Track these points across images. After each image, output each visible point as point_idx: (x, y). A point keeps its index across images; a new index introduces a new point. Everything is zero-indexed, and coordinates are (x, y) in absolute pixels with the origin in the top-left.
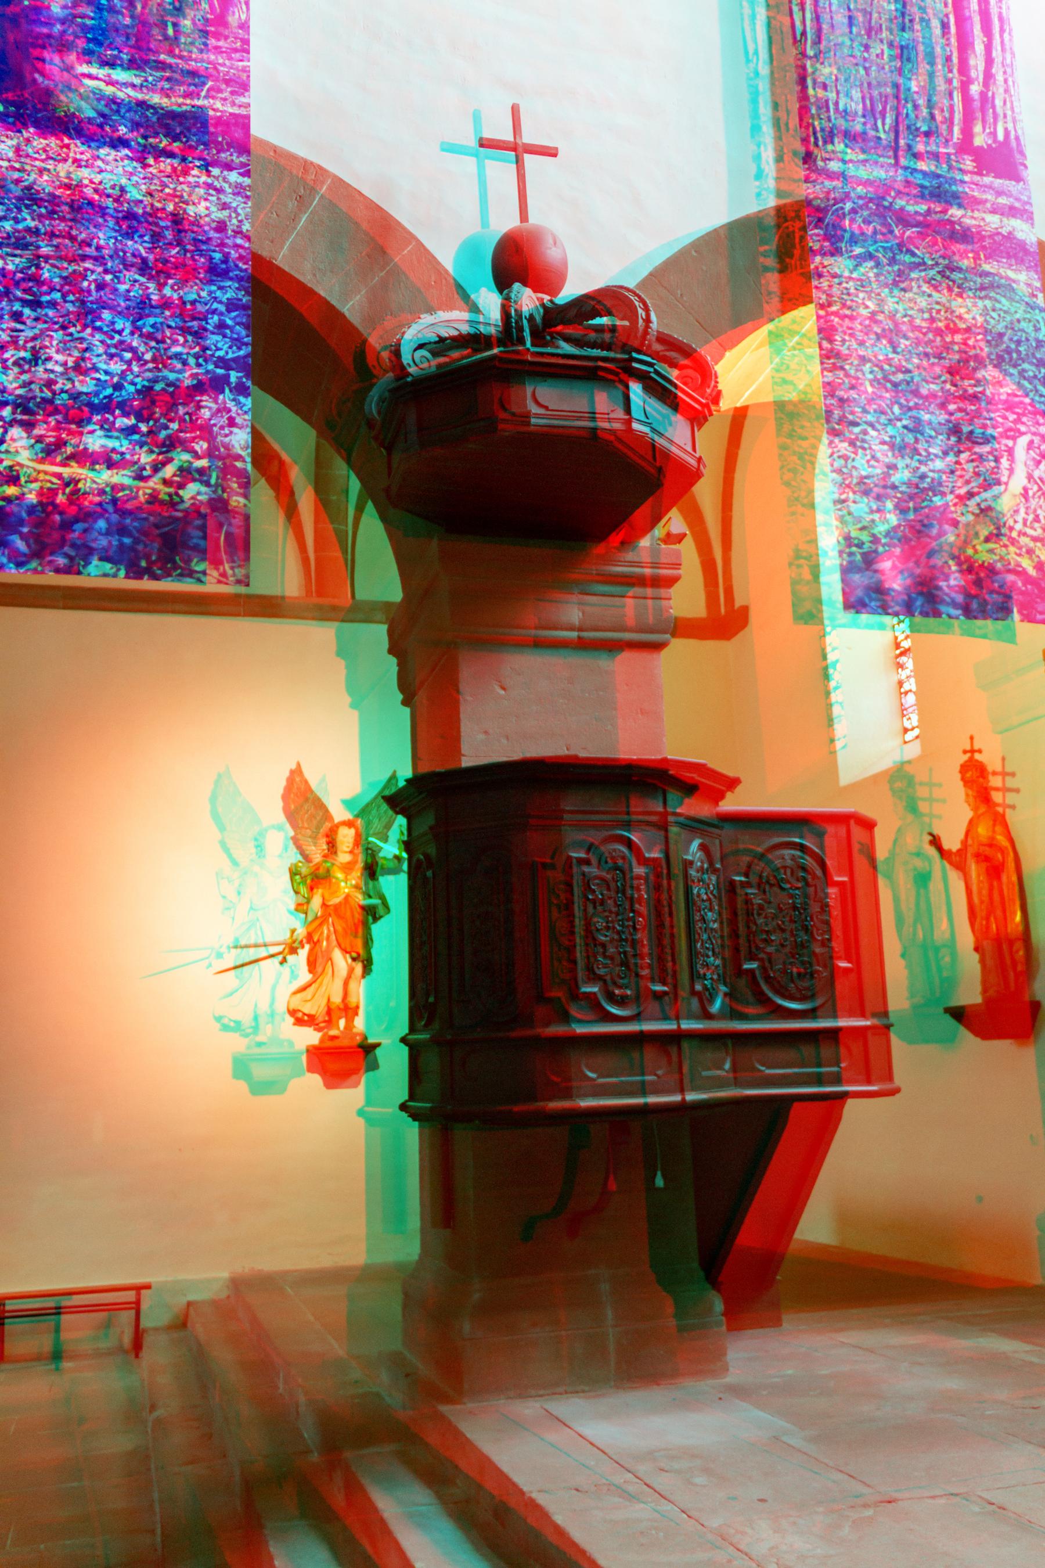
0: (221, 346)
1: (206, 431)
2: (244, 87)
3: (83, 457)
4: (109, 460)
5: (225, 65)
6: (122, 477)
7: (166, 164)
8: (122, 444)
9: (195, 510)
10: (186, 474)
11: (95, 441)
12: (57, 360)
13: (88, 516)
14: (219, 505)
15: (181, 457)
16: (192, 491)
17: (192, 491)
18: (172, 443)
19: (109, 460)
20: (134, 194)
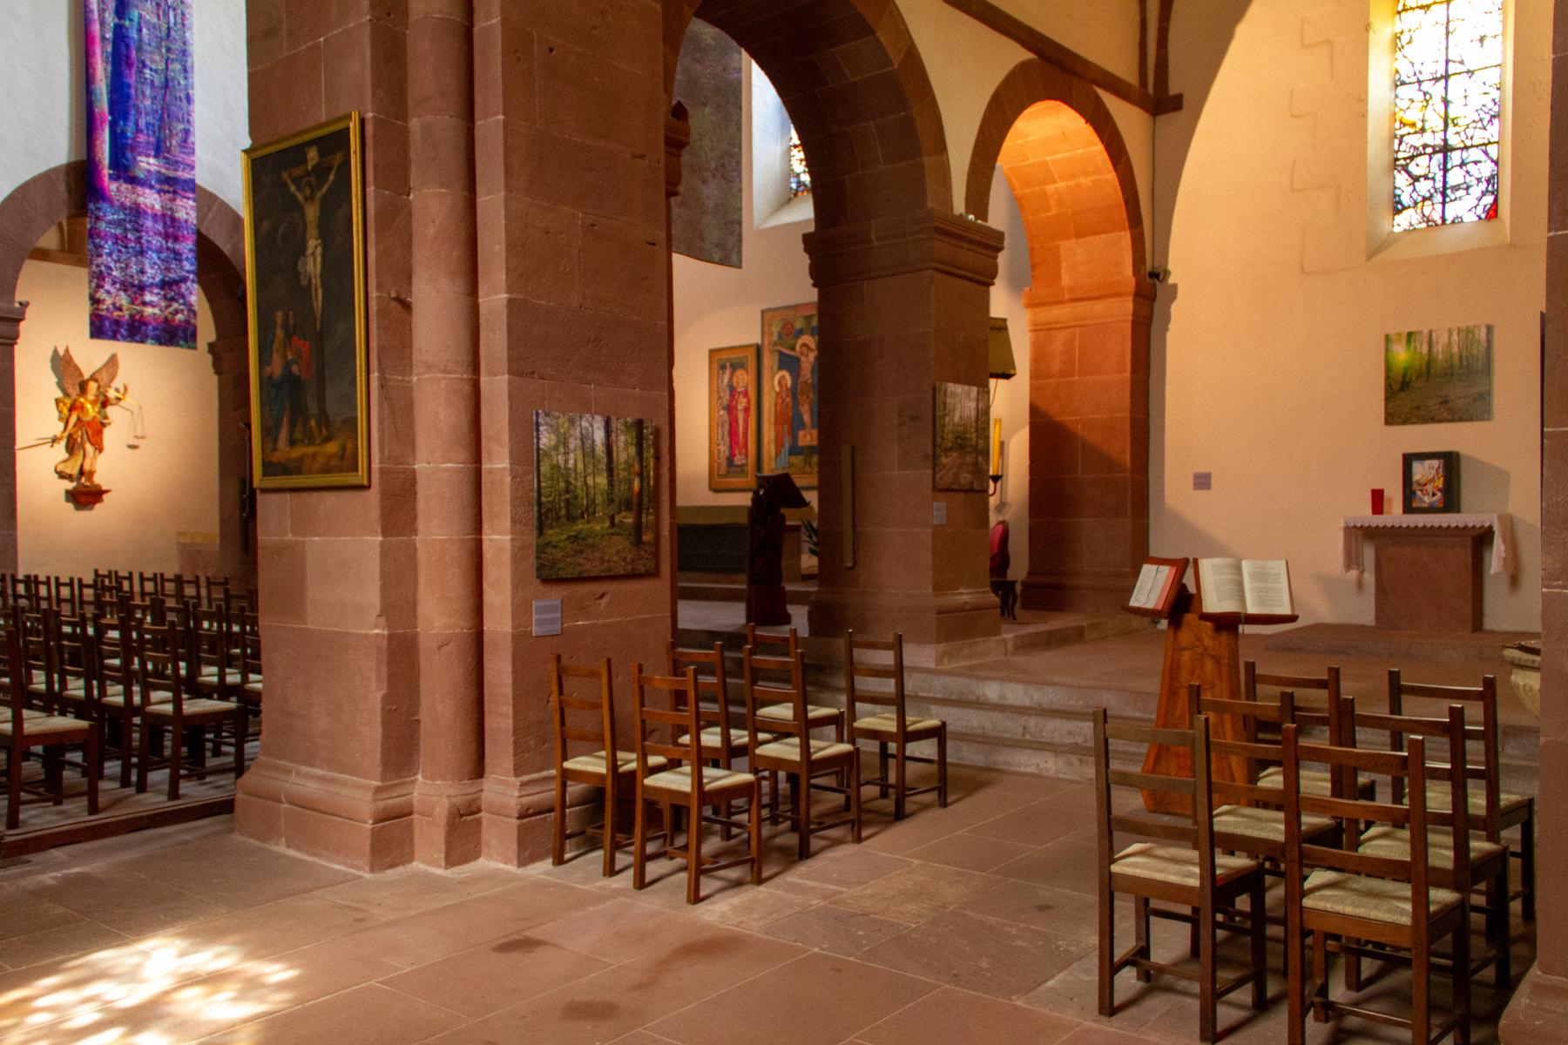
0: (187, 266)
1: (183, 296)
2: (193, 168)
3: (145, 304)
4: (151, 304)
5: (188, 159)
6: (157, 311)
7: (168, 196)
8: (155, 299)
9: (178, 326)
10: (177, 312)
11: (148, 297)
12: (134, 269)
13: (146, 324)
14: (187, 322)
15: (175, 305)
16: (179, 317)
17: (179, 317)
18: (173, 299)
19: (151, 304)
20: (158, 207)
